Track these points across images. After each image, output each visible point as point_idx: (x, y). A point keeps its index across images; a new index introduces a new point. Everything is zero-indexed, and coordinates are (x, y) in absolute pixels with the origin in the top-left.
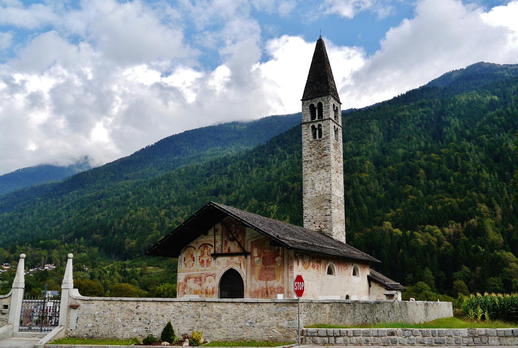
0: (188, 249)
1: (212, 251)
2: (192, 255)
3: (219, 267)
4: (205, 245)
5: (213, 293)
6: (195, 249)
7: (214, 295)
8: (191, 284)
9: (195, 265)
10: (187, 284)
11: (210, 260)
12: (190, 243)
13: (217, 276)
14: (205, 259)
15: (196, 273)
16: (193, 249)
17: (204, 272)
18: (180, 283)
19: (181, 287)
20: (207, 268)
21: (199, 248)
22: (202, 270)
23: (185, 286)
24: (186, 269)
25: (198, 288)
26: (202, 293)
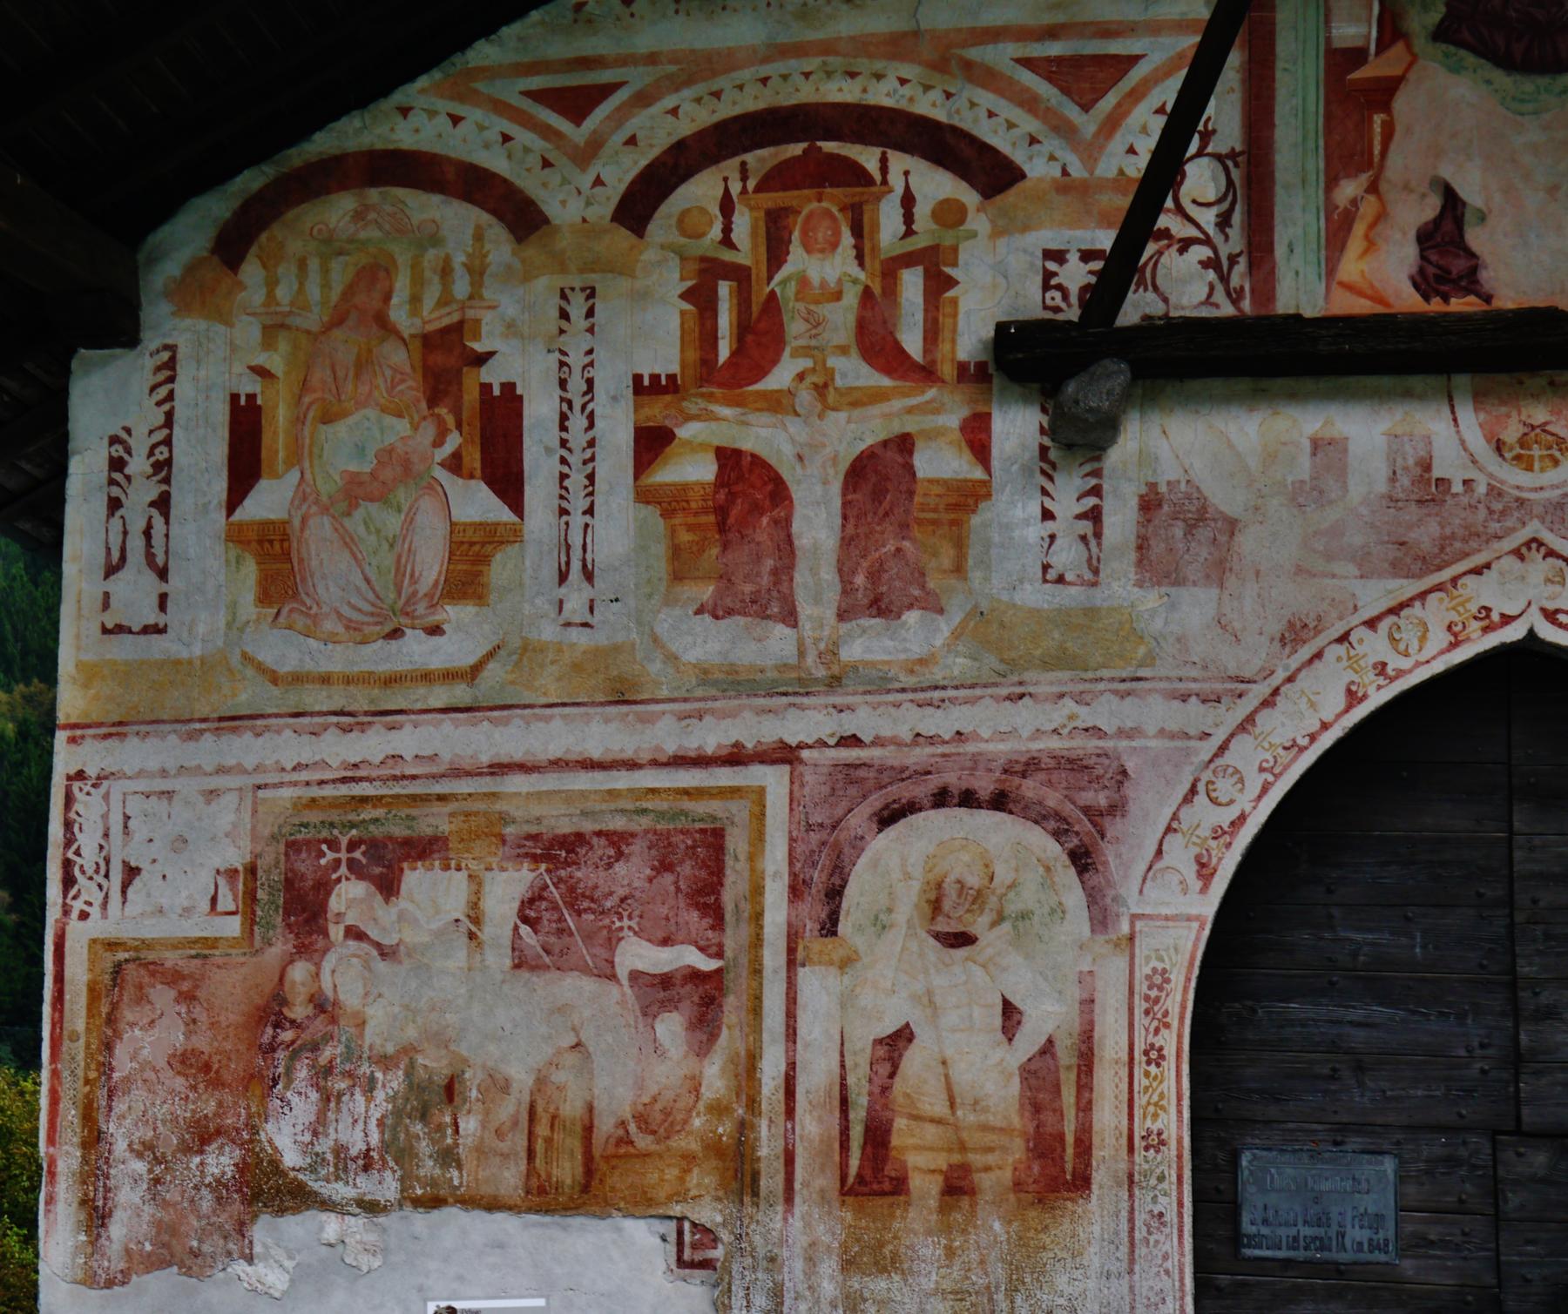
0: (337, 211)
1: (1003, 277)
2: (447, 358)
3: (1185, 616)
4: (809, 151)
5: (1057, 1171)
6: (522, 217)
7: (1097, 1217)
8: (435, 968)
9: (522, 570)
10: (341, 973)
11: (939, 462)
12: (374, 83)
13: (1151, 805)
14: (810, 451)
15: (565, 758)
16: (457, 220)
17: (803, 724)
18: (127, 972)
19: (152, 1037)
20: (867, 644)
21: (636, 209)
22: (734, 684)
23: (277, 1036)
24: (282, 649)
25: (639, 1068)
26: (739, 1173)
